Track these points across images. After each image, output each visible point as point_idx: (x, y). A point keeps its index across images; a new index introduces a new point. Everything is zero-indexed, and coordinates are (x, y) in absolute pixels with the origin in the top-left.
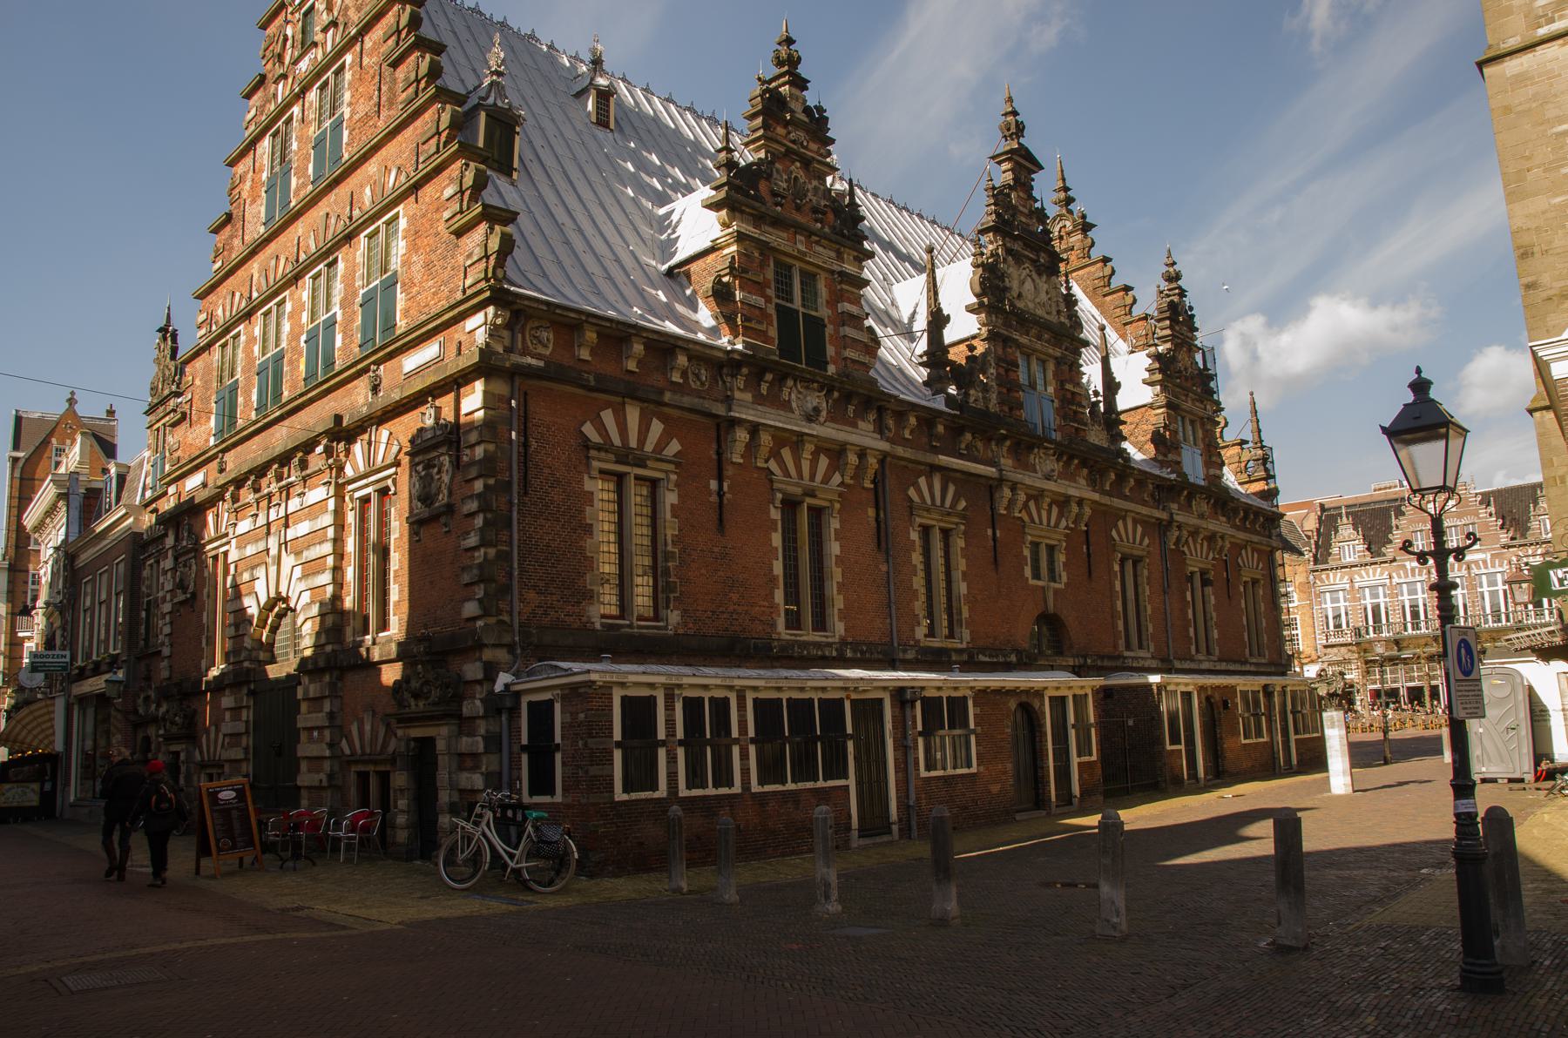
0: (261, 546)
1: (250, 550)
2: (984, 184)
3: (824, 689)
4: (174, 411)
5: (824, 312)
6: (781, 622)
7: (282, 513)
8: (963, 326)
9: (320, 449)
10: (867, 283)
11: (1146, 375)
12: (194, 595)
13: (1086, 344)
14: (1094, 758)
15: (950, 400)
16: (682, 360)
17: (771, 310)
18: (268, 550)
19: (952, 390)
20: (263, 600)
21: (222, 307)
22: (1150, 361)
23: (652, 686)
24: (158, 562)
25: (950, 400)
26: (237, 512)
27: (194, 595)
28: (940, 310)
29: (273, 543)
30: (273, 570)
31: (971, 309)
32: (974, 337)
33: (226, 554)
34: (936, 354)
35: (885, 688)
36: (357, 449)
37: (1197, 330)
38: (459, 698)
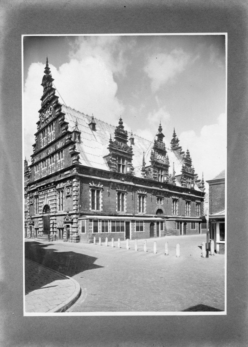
0: (44, 197)
1: (42, 197)
2: (154, 140)
3: (121, 220)
4: (28, 174)
5: (125, 164)
6: (117, 210)
7: (47, 193)
8: (148, 164)
9: (53, 184)
10: (132, 159)
11: (181, 170)
12: (33, 204)
13: (170, 166)
14: (164, 230)
15: (145, 177)
16: (103, 173)
17: (117, 164)
18: (45, 198)
19: (146, 175)
20: (44, 205)
21: (36, 160)
22: (182, 168)
23: (97, 219)
24: (26, 198)
25: (145, 177)
26: (40, 192)
27: (33, 204)
28: (145, 163)
29: (46, 196)
30: (46, 201)
31: (150, 162)
32: (150, 166)
33: (38, 198)
34: (144, 170)
35: (130, 220)
36: (58, 185)
37: (192, 162)
38: (72, 220)
